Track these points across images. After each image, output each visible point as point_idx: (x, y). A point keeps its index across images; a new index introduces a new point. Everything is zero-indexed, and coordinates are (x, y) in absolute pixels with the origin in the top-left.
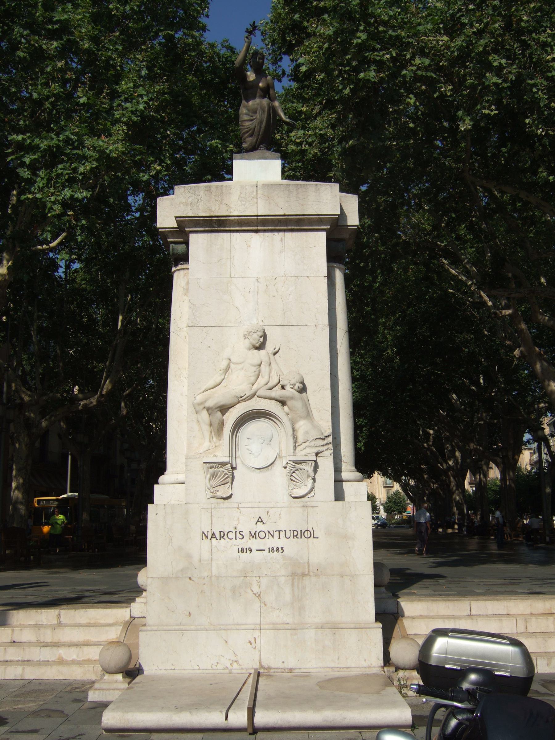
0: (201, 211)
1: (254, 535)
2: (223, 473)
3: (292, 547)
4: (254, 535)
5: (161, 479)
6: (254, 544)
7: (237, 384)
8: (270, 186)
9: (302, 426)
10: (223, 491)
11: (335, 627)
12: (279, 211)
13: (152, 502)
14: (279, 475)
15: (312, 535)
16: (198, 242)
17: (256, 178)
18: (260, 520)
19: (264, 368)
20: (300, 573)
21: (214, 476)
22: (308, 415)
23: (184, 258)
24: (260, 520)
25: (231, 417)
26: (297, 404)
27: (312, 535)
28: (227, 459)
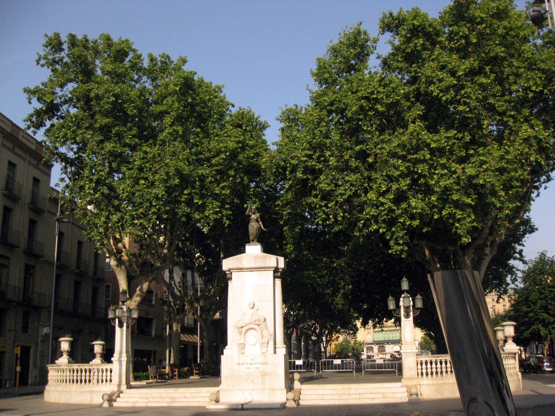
0: (235, 266)
1: (251, 364)
2: (242, 346)
3: (261, 367)
4: (251, 364)
5: (226, 347)
6: (251, 366)
7: (247, 319)
8: (257, 257)
9: (265, 332)
10: (242, 351)
11: (273, 389)
12: (258, 266)
13: (223, 354)
14: (258, 346)
15: (267, 364)
16: (235, 275)
17: (254, 250)
18: (253, 360)
19: (254, 315)
20: (264, 375)
21: (239, 347)
22: (267, 328)
23: (231, 279)
24: (253, 360)
25: (244, 330)
26: (263, 326)
27: (267, 364)
28: (243, 342)
